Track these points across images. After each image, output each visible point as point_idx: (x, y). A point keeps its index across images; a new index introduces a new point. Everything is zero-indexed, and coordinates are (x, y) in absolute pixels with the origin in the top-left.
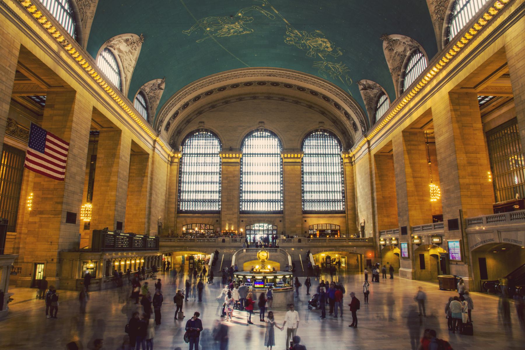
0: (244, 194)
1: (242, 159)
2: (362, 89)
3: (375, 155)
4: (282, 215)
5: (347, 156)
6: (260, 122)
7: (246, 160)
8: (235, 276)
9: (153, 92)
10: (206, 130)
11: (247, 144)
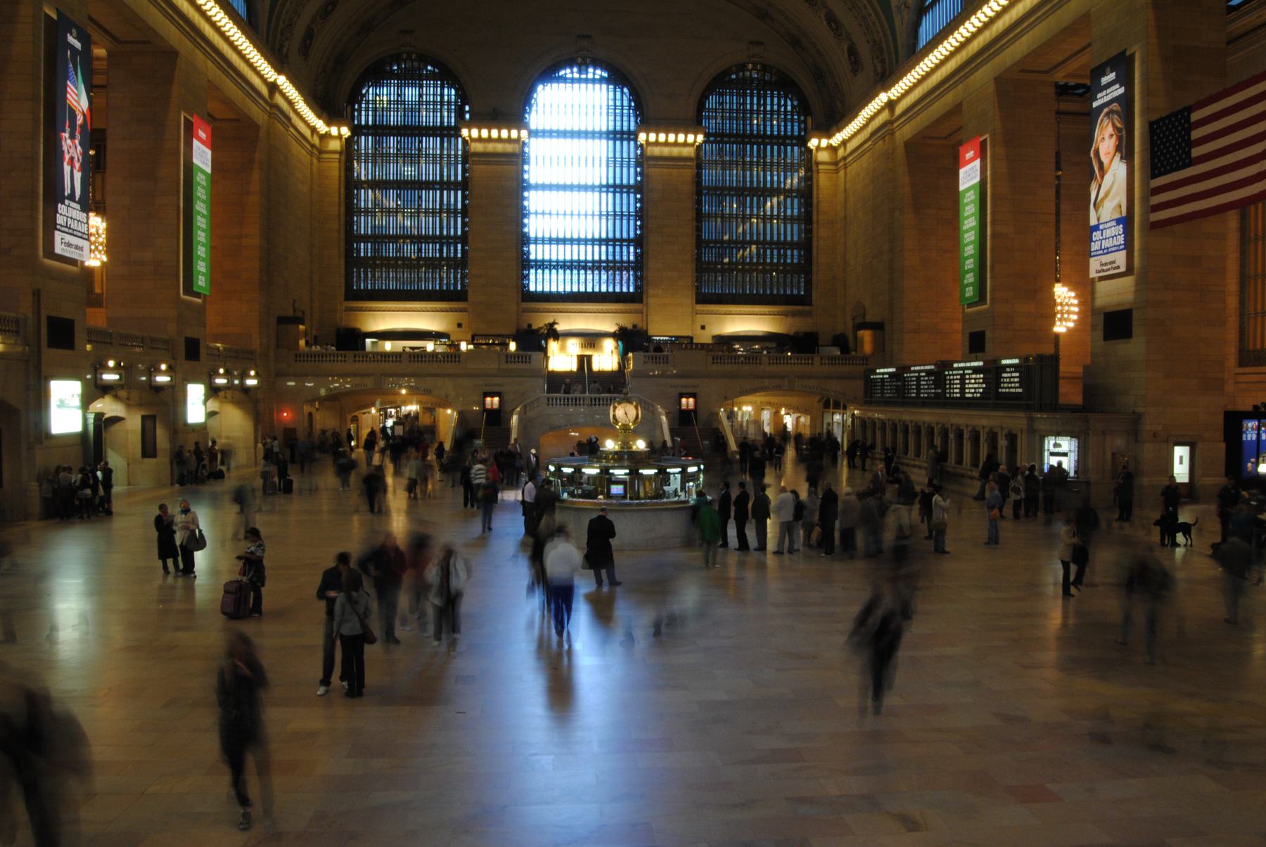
0: (532, 247)
3: (909, 145)
7: (536, 148)
8: (552, 468)
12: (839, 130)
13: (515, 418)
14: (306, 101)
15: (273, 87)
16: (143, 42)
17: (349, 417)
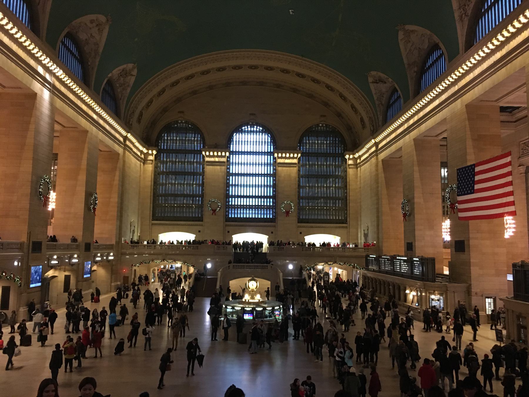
0: (230, 199)
1: (229, 157)
2: (373, 82)
3: (383, 160)
4: (273, 224)
5: (351, 157)
6: (251, 114)
9: (122, 79)
10: (186, 122)
11: (234, 140)
12: (358, 152)
13: (219, 273)
14: (139, 142)
15: (126, 138)
16: (74, 127)
17: (152, 270)
